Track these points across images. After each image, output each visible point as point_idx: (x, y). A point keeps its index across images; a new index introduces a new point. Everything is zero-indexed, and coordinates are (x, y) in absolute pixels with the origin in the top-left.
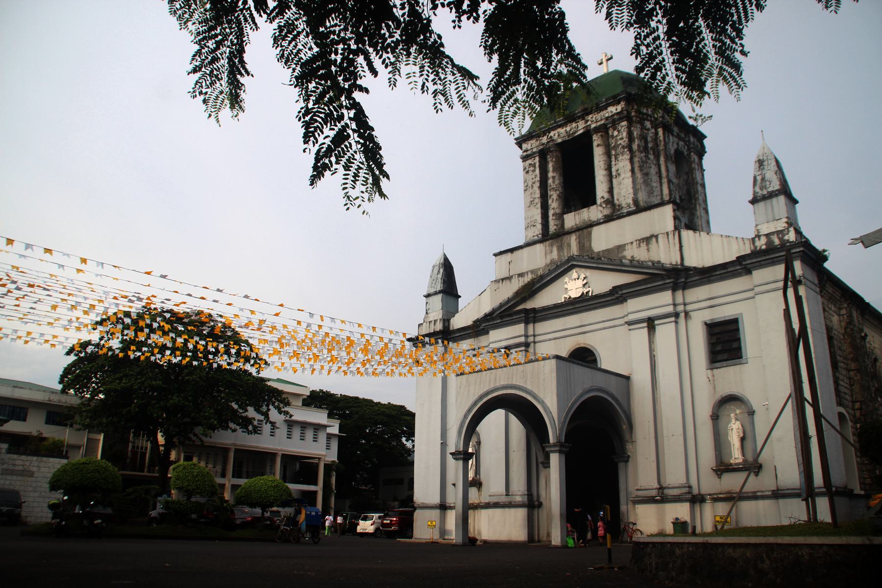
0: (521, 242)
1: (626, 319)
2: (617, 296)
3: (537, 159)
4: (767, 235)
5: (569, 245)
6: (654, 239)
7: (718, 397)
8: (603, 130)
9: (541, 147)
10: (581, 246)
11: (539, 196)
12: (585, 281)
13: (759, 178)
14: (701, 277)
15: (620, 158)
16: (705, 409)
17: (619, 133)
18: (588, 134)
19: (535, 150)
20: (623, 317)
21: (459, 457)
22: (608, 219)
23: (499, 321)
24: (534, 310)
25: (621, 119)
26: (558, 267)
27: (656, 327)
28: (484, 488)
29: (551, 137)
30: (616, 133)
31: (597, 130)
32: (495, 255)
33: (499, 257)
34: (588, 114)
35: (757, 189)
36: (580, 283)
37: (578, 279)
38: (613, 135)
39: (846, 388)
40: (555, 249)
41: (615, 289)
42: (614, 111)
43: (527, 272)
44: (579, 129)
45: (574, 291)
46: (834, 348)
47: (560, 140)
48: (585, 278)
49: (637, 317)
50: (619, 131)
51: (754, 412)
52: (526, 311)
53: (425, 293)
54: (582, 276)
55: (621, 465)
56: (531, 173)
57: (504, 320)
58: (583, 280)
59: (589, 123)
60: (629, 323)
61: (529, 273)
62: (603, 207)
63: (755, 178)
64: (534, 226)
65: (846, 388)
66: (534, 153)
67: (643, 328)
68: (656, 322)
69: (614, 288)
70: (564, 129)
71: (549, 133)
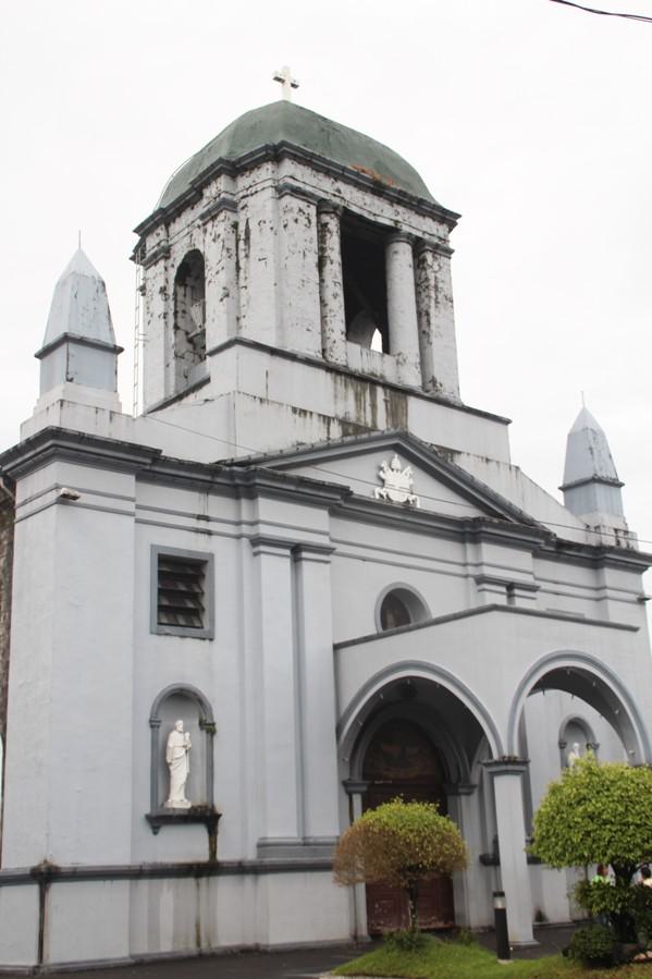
2: (465, 533)
4: (616, 530)
5: (374, 406)
9: (323, 195)
18: (390, 233)
23: (292, 488)
24: (345, 492)
29: (339, 191)
34: (399, 202)
42: (435, 232)
47: (354, 209)
49: (270, 533)
50: (440, 268)
57: (301, 490)
61: (315, 417)
64: (308, 330)
66: (312, 196)
67: (502, 593)
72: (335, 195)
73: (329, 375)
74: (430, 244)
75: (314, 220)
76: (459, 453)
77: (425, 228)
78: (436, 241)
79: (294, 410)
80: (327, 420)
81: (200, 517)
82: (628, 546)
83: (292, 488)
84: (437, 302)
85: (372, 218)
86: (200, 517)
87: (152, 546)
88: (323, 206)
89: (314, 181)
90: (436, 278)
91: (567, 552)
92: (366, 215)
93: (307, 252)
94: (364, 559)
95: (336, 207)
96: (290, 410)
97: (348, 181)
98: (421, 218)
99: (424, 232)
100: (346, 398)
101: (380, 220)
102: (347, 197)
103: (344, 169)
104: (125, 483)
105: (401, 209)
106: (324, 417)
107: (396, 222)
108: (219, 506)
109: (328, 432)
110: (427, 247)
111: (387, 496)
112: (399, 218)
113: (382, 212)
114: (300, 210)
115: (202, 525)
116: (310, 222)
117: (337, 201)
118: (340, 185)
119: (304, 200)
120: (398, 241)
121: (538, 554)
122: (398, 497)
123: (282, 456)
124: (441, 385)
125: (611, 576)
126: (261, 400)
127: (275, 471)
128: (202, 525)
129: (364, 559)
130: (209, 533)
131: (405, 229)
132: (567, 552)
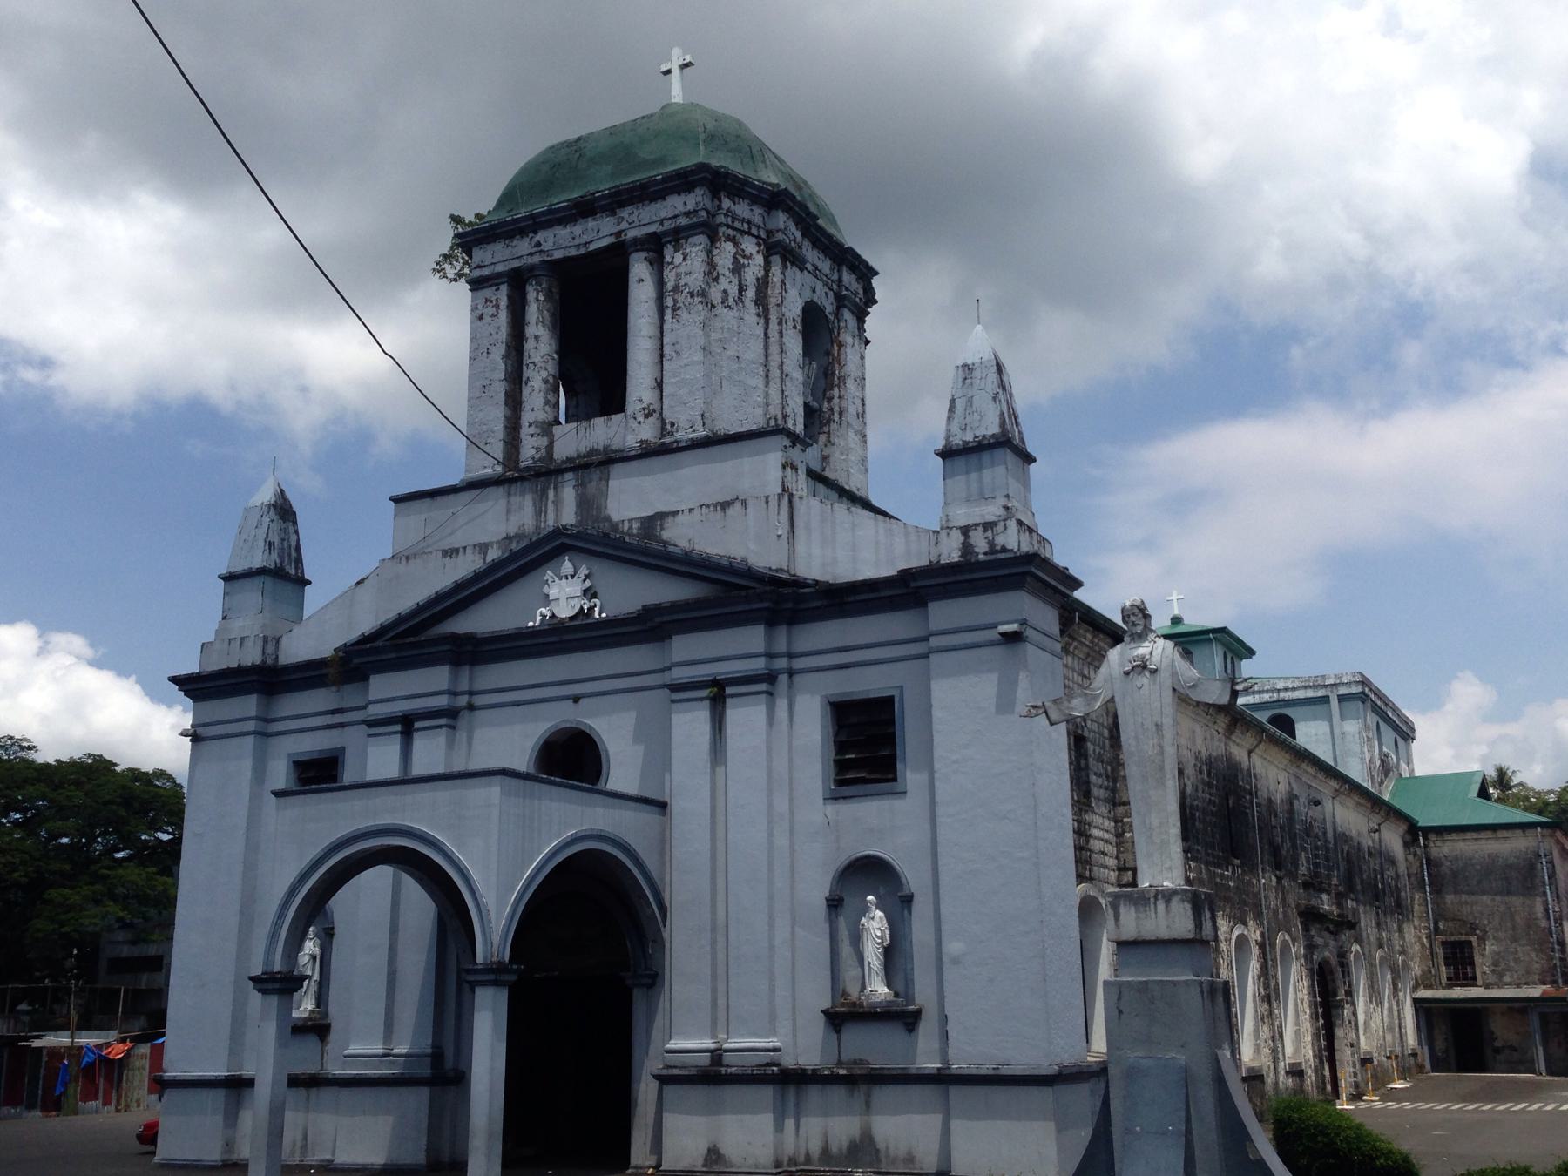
0: (454, 480)
1: (667, 678)
3: (504, 289)
4: (965, 531)
5: (558, 502)
6: (738, 505)
7: (843, 859)
8: (655, 246)
9: (516, 264)
10: (586, 504)
11: (502, 376)
12: (588, 583)
13: (960, 404)
14: (825, 602)
15: (683, 314)
16: (816, 887)
17: (684, 259)
19: (500, 268)
20: (662, 671)
21: (270, 986)
22: (648, 452)
23: (393, 655)
24: (471, 638)
25: (694, 229)
26: (533, 546)
27: (727, 700)
28: (333, 1036)
29: (539, 244)
30: (679, 257)
31: (640, 244)
32: (397, 500)
33: (402, 505)
34: (622, 205)
35: (955, 429)
36: (575, 587)
37: (573, 577)
38: (672, 263)
39: (1107, 841)
40: (528, 501)
41: (649, 612)
42: (681, 209)
43: (465, 548)
44: (601, 235)
45: (563, 602)
46: (1086, 759)
47: (558, 255)
48: (587, 577)
51: (911, 896)
52: (455, 638)
53: (224, 571)
54: (583, 571)
55: (638, 996)
56: (487, 319)
58: (584, 581)
59: (624, 225)
60: (675, 688)
61: (469, 550)
62: (639, 423)
63: (953, 401)
64: (486, 444)
65: (1107, 841)
66: (499, 275)
67: (701, 699)
68: (729, 690)
69: (645, 608)
70: (568, 229)
71: (535, 232)
72: (531, 254)
73: (501, 489)
74: (666, 233)
75: (504, 302)
76: (675, 513)
77: (663, 215)
78: (668, 225)
79: (445, 553)
80: (483, 548)
81: (334, 712)
82: (992, 544)
83: (393, 655)
84: (675, 309)
85: (582, 251)
86: (334, 712)
87: (343, 749)
88: (517, 280)
89: (507, 253)
90: (678, 274)
91: (851, 599)
92: (573, 252)
93: (492, 349)
94: (517, 704)
95: (532, 268)
96: (440, 554)
97: (548, 225)
98: (658, 205)
99: (662, 222)
100: (522, 507)
101: (592, 247)
102: (546, 247)
103: (532, 217)
104: (248, 705)
105: (624, 213)
106: (480, 545)
107: (618, 234)
108: (349, 696)
109: (484, 559)
110: (664, 240)
111: (553, 616)
112: (624, 225)
113: (598, 233)
114: (487, 300)
115: (338, 719)
116: (497, 306)
117: (537, 259)
118: (540, 236)
119: (490, 286)
120: (631, 253)
121: (772, 620)
122: (565, 611)
123: (401, 619)
124: (673, 424)
125: (943, 614)
126: (407, 558)
127: (363, 647)
128: (338, 719)
129: (517, 704)
130: (342, 725)
131: (631, 234)
132: (851, 599)
